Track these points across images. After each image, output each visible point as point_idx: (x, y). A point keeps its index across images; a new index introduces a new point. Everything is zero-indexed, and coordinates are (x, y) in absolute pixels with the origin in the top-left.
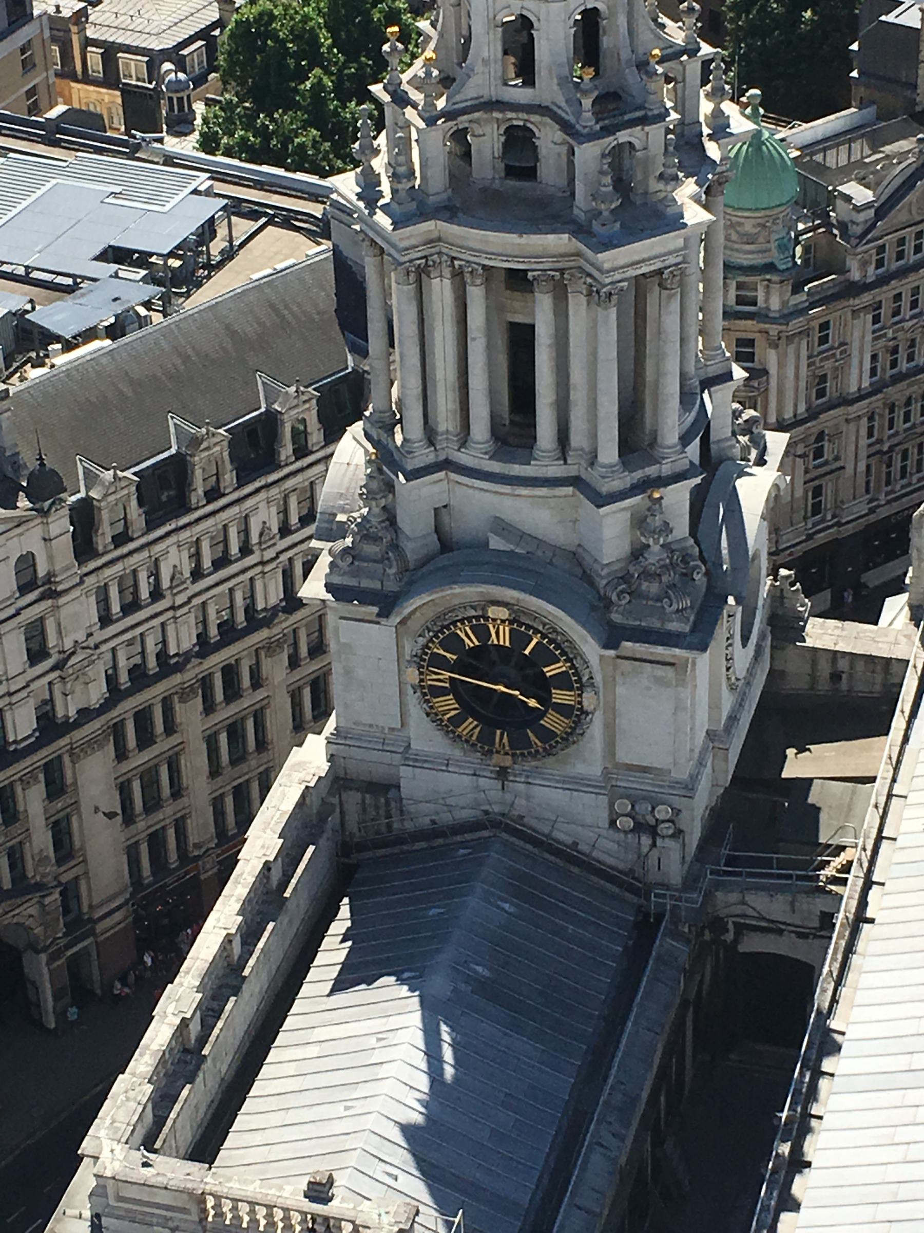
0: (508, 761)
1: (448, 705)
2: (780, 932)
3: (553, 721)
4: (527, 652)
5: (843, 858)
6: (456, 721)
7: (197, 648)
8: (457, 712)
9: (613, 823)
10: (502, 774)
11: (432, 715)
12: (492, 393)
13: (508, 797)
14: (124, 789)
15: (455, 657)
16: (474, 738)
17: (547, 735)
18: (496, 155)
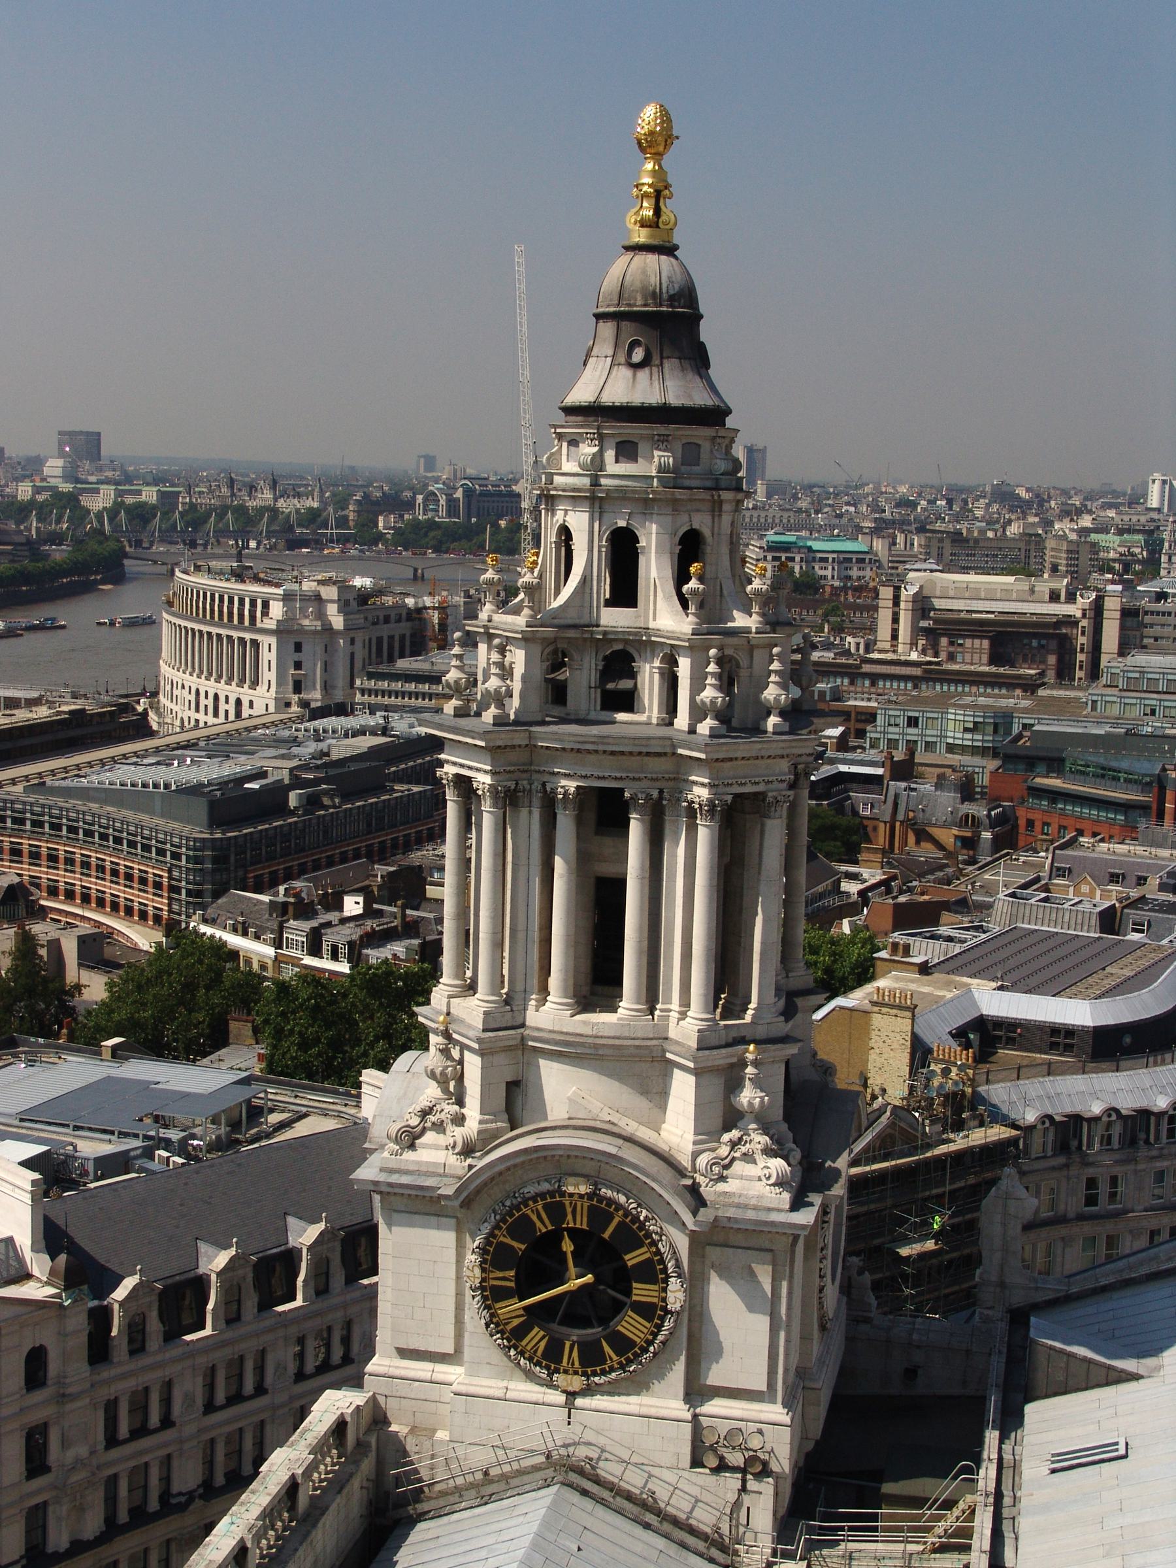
0: (577, 1383)
3: (631, 1325)
4: (606, 1235)
7: (201, 1491)
8: (522, 1319)
11: (495, 1324)
15: (523, 1247)
16: (539, 1353)
17: (623, 1344)
18: (593, 685)
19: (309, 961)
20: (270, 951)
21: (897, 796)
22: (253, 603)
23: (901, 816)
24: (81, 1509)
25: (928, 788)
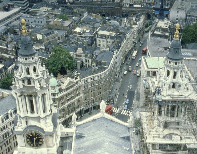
0: (36, 148)
1: (30, 143)
3: (40, 143)
6: (31, 144)
11: (28, 144)
17: (40, 145)
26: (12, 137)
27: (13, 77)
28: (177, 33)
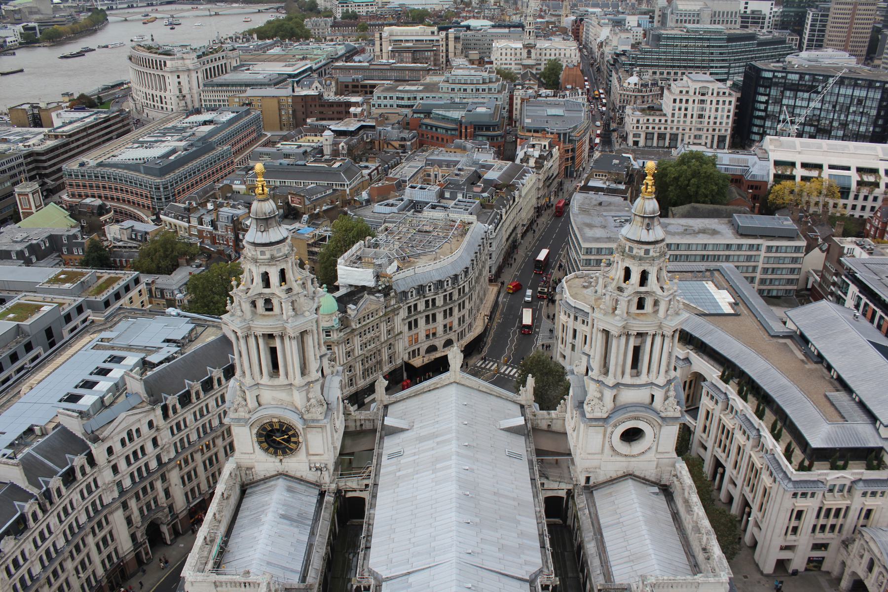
0: (282, 457)
1: (265, 445)
2: (355, 491)
3: (292, 446)
5: (369, 469)
9: (310, 469)
10: (281, 460)
11: (262, 448)
12: (267, 365)
13: (283, 467)
14: (182, 478)
17: (291, 450)
19: (200, 227)
20: (187, 225)
21: (380, 132)
22: (160, 61)
23: (382, 138)
24: (168, 452)
25: (389, 128)
26: (219, 433)
27: (229, 295)
28: (650, 183)
